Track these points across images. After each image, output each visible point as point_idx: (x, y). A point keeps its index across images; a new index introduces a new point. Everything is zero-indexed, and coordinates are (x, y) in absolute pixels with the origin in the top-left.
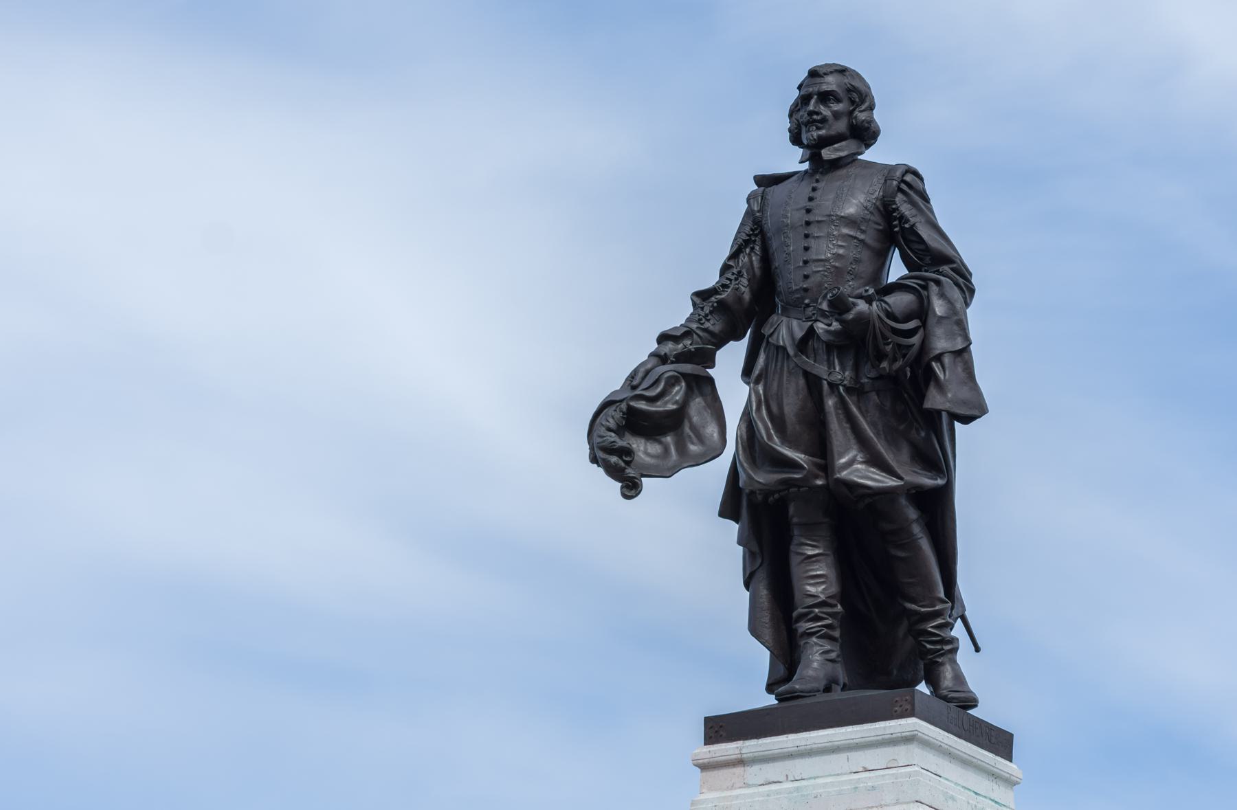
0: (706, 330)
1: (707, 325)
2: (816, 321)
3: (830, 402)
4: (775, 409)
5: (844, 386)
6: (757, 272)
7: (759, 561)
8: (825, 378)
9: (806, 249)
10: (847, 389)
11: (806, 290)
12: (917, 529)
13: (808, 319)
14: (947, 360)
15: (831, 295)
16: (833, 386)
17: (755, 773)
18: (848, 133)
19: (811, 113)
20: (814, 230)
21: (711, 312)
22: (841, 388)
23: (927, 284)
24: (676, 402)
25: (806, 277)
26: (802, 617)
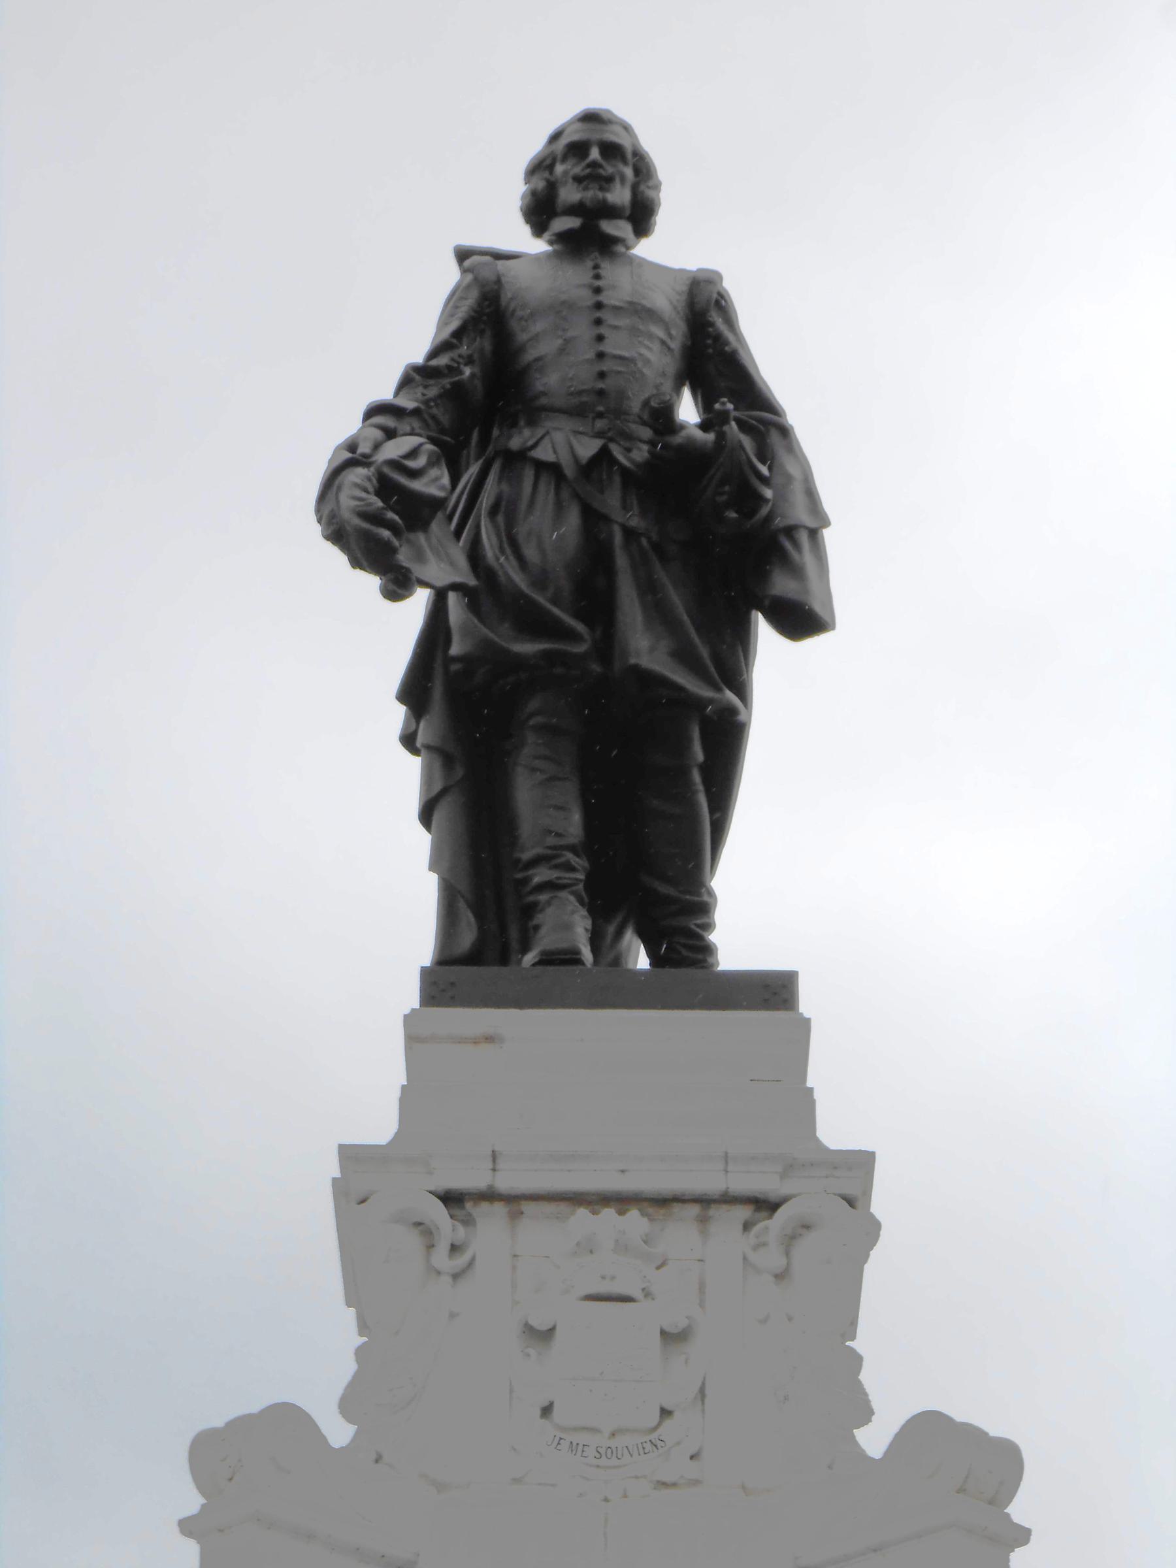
0: (433, 417)
1: (435, 411)
2: (611, 440)
4: (531, 553)
5: (649, 539)
7: (460, 772)
8: (620, 520)
9: (600, 338)
11: (601, 393)
12: (697, 777)
13: (599, 435)
15: (657, 401)
16: (630, 534)
18: (628, 212)
19: (594, 165)
21: (440, 396)
22: (644, 541)
23: (768, 431)
24: (442, 488)
25: (602, 375)
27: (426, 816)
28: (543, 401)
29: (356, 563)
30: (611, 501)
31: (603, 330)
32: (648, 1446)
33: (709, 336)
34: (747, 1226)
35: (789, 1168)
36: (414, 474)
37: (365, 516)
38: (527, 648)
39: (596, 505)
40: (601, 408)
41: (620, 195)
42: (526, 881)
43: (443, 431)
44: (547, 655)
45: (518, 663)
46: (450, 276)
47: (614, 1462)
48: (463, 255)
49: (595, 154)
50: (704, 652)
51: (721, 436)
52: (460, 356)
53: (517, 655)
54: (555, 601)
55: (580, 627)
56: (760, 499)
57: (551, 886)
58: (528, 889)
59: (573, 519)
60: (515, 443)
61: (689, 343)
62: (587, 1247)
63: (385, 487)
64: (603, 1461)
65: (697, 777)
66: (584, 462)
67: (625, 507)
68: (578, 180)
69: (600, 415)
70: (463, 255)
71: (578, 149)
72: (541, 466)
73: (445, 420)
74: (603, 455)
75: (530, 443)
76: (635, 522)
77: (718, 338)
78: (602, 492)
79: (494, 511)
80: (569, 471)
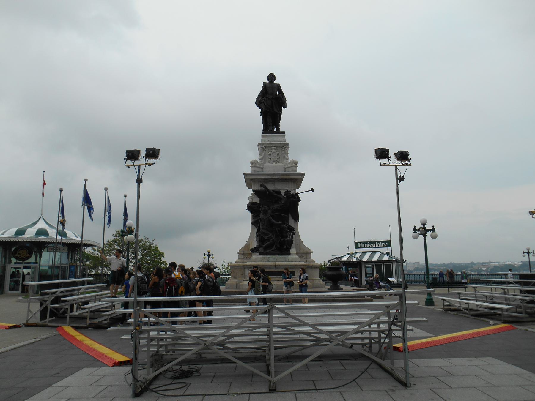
12: (279, 118)
17: (268, 137)
27: (262, 121)
35: (284, 144)
36: (261, 100)
37: (258, 104)
41: (273, 79)
46: (263, 84)
48: (263, 83)
49: (272, 76)
50: (279, 110)
56: (282, 100)
60: (267, 96)
62: (273, 149)
65: (279, 118)
68: (271, 78)
70: (263, 83)
71: (270, 76)
72: (269, 98)
77: (280, 89)
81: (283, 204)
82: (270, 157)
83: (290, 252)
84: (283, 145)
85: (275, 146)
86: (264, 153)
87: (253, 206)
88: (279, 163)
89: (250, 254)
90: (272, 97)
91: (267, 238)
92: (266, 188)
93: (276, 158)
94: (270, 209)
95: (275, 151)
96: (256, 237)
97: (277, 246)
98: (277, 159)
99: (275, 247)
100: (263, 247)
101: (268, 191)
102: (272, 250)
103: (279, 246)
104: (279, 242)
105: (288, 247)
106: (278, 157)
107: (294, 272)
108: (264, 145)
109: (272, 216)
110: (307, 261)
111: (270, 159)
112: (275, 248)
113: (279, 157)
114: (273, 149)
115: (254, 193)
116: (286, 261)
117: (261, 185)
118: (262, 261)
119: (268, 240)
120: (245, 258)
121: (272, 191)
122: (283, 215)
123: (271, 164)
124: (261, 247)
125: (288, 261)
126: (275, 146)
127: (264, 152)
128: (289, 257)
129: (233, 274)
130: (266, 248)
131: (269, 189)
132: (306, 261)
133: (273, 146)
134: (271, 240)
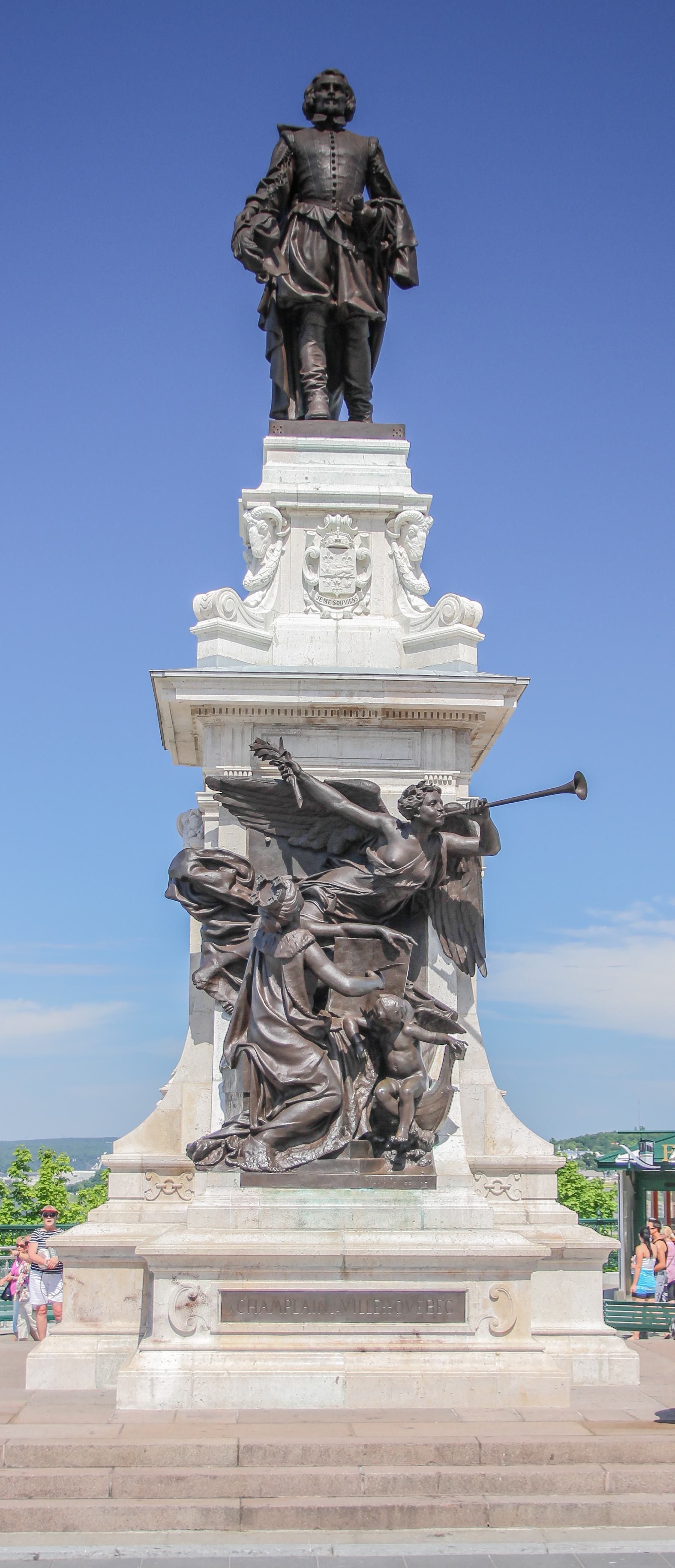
0: (272, 201)
1: (273, 199)
2: (338, 211)
3: (342, 260)
4: (308, 256)
5: (352, 251)
6: (292, 178)
10: (353, 254)
11: (334, 192)
13: (334, 209)
14: (406, 249)
16: (345, 250)
19: (331, 94)
20: (336, 159)
21: (274, 192)
23: (396, 206)
26: (312, 376)
28: (312, 194)
29: (246, 268)
30: (337, 235)
31: (335, 165)
32: (351, 601)
33: (374, 166)
34: (386, 521)
36: (268, 231)
38: (306, 294)
39: (332, 238)
40: (334, 198)
42: (306, 384)
43: (274, 206)
44: (314, 298)
45: (303, 301)
47: (340, 606)
51: (379, 212)
52: (281, 174)
53: (303, 298)
54: (317, 276)
55: (325, 286)
57: (315, 386)
58: (305, 388)
59: (323, 243)
61: (366, 169)
63: (257, 238)
64: (336, 606)
66: (328, 220)
67: (343, 238)
69: (334, 201)
73: (276, 202)
74: (335, 216)
75: (308, 211)
76: (346, 245)
78: (335, 231)
79: (294, 238)
80: (323, 224)
81: (393, 865)
82: (311, 577)
83: (430, 1165)
84: (395, 507)
85: (343, 512)
86: (277, 553)
87: (213, 875)
88: (366, 614)
89: (181, 1170)
90: (330, 214)
91: (298, 1076)
92: (289, 765)
93: (349, 582)
94: (308, 896)
95: (344, 540)
96: (222, 1070)
97: (354, 1125)
98: (358, 589)
99: (342, 1133)
100: (266, 1134)
101: (301, 783)
102: (321, 1151)
103: (365, 1128)
104: (363, 1100)
105: (418, 1129)
106: (362, 579)
107: (460, 1295)
108: (280, 503)
109: (322, 939)
110: (532, 1220)
111: (316, 588)
112: (342, 1143)
113: (369, 582)
114: (333, 527)
115: (216, 797)
116: (404, 1226)
117: (261, 750)
118: (258, 1224)
119: (300, 1088)
120: (151, 1195)
121: (326, 782)
122: (389, 933)
123: (314, 619)
124: (255, 1133)
125: (423, 1229)
126: (343, 512)
127: (280, 542)
128: (427, 1199)
129: (76, 1296)
130: (282, 1143)
131: (305, 775)
132: (527, 1215)
133: (333, 512)
134: (318, 1089)
